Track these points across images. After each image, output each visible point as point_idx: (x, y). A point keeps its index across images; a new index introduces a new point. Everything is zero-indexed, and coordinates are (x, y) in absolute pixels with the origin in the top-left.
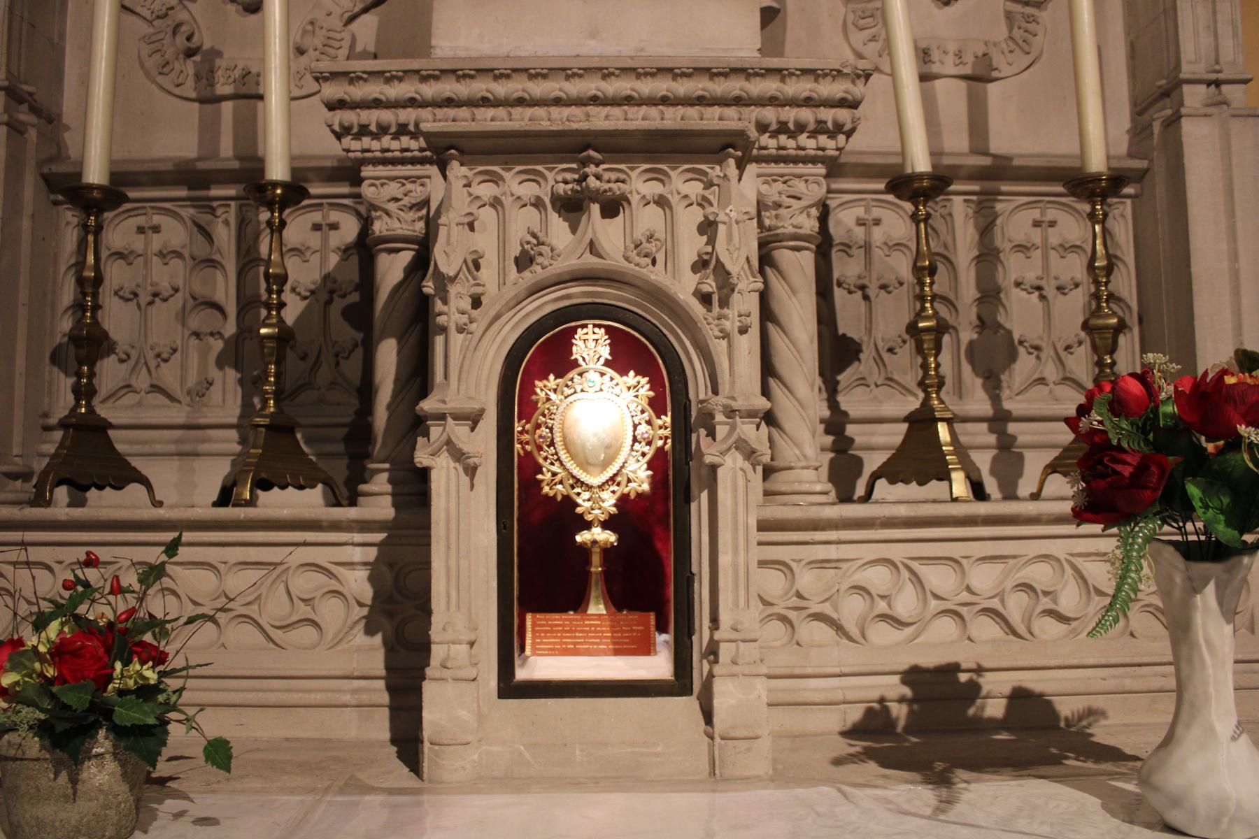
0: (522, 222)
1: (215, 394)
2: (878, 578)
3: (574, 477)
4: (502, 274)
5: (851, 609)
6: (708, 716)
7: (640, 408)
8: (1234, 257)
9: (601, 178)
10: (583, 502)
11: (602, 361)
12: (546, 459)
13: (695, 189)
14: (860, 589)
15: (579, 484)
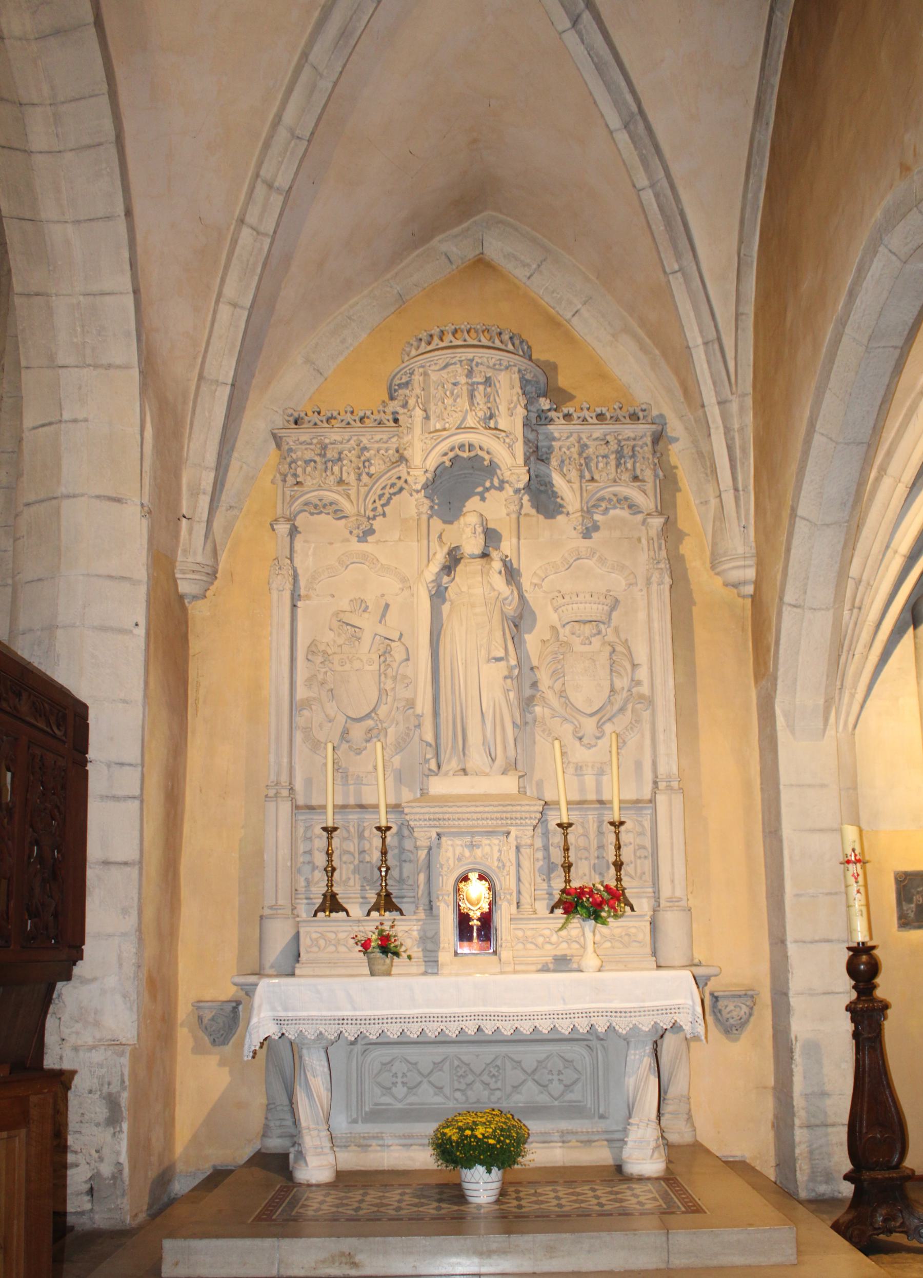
0: (459, 850)
1: (351, 883)
2: (547, 932)
4: (454, 862)
5: (540, 940)
6: (500, 960)
8: (672, 838)
9: (477, 838)
10: (471, 914)
13: (496, 842)
14: (542, 935)
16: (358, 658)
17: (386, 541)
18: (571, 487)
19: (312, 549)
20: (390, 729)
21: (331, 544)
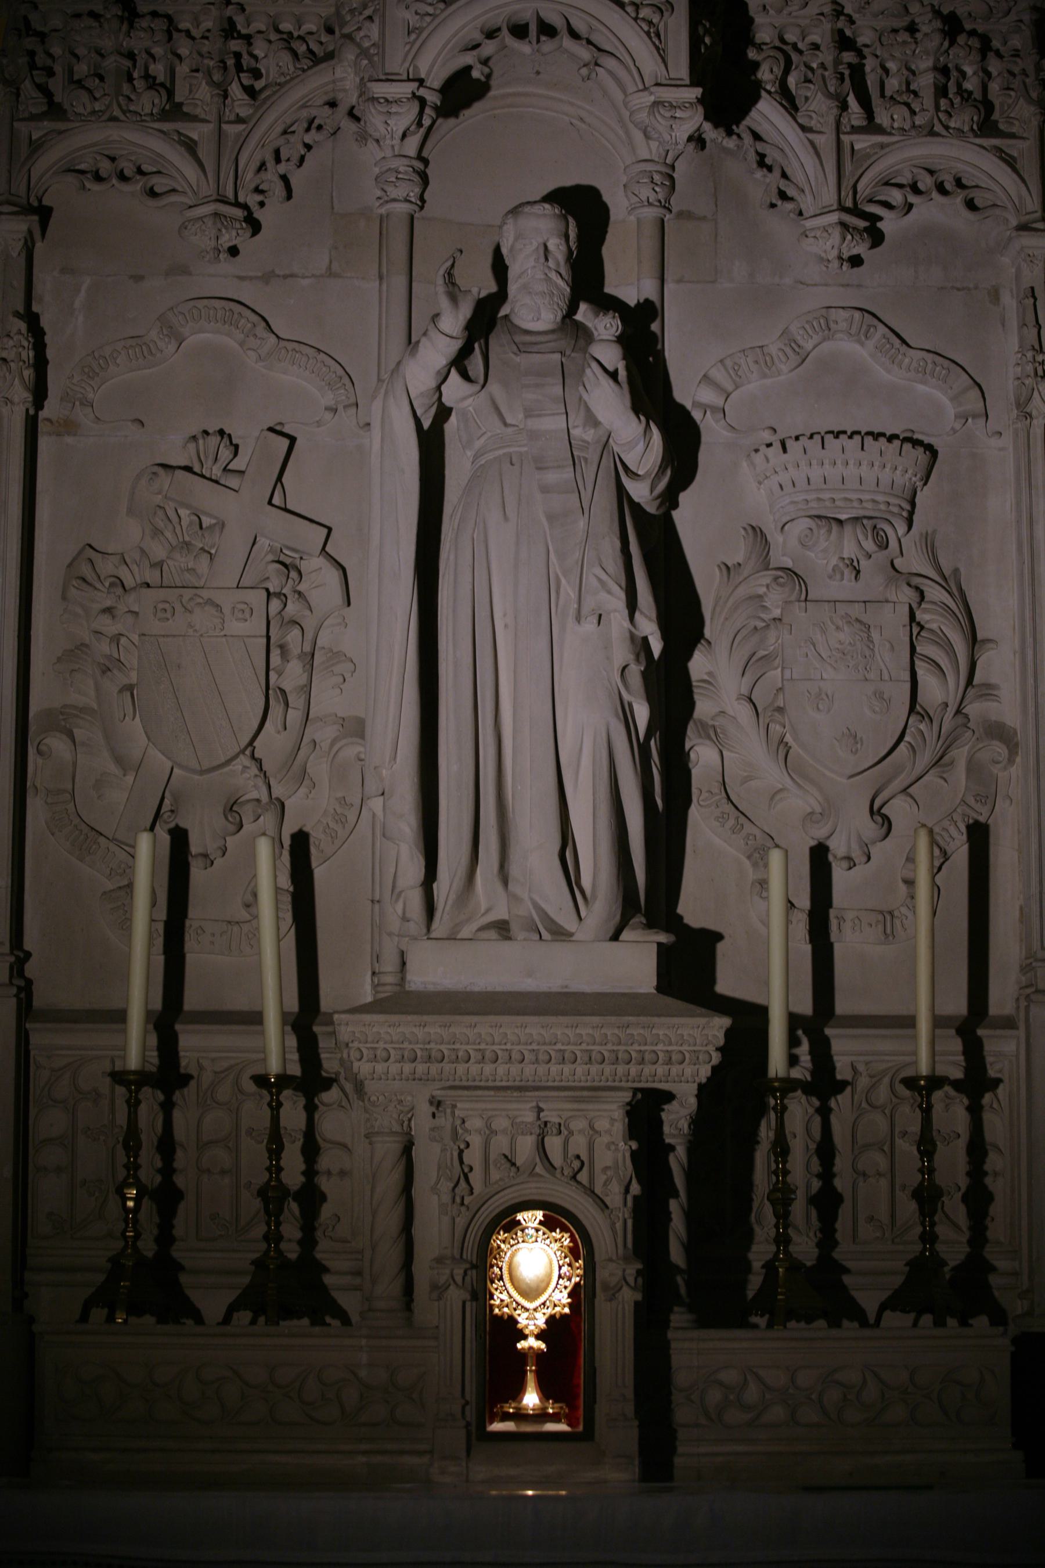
3: (517, 1303)
7: (563, 1255)
10: (522, 1320)
11: (537, 1221)
12: (496, 1289)
15: (520, 1307)
16: (210, 602)
17: (292, 276)
18: (812, 143)
19: (83, 293)
20: (293, 799)
21: (138, 278)
